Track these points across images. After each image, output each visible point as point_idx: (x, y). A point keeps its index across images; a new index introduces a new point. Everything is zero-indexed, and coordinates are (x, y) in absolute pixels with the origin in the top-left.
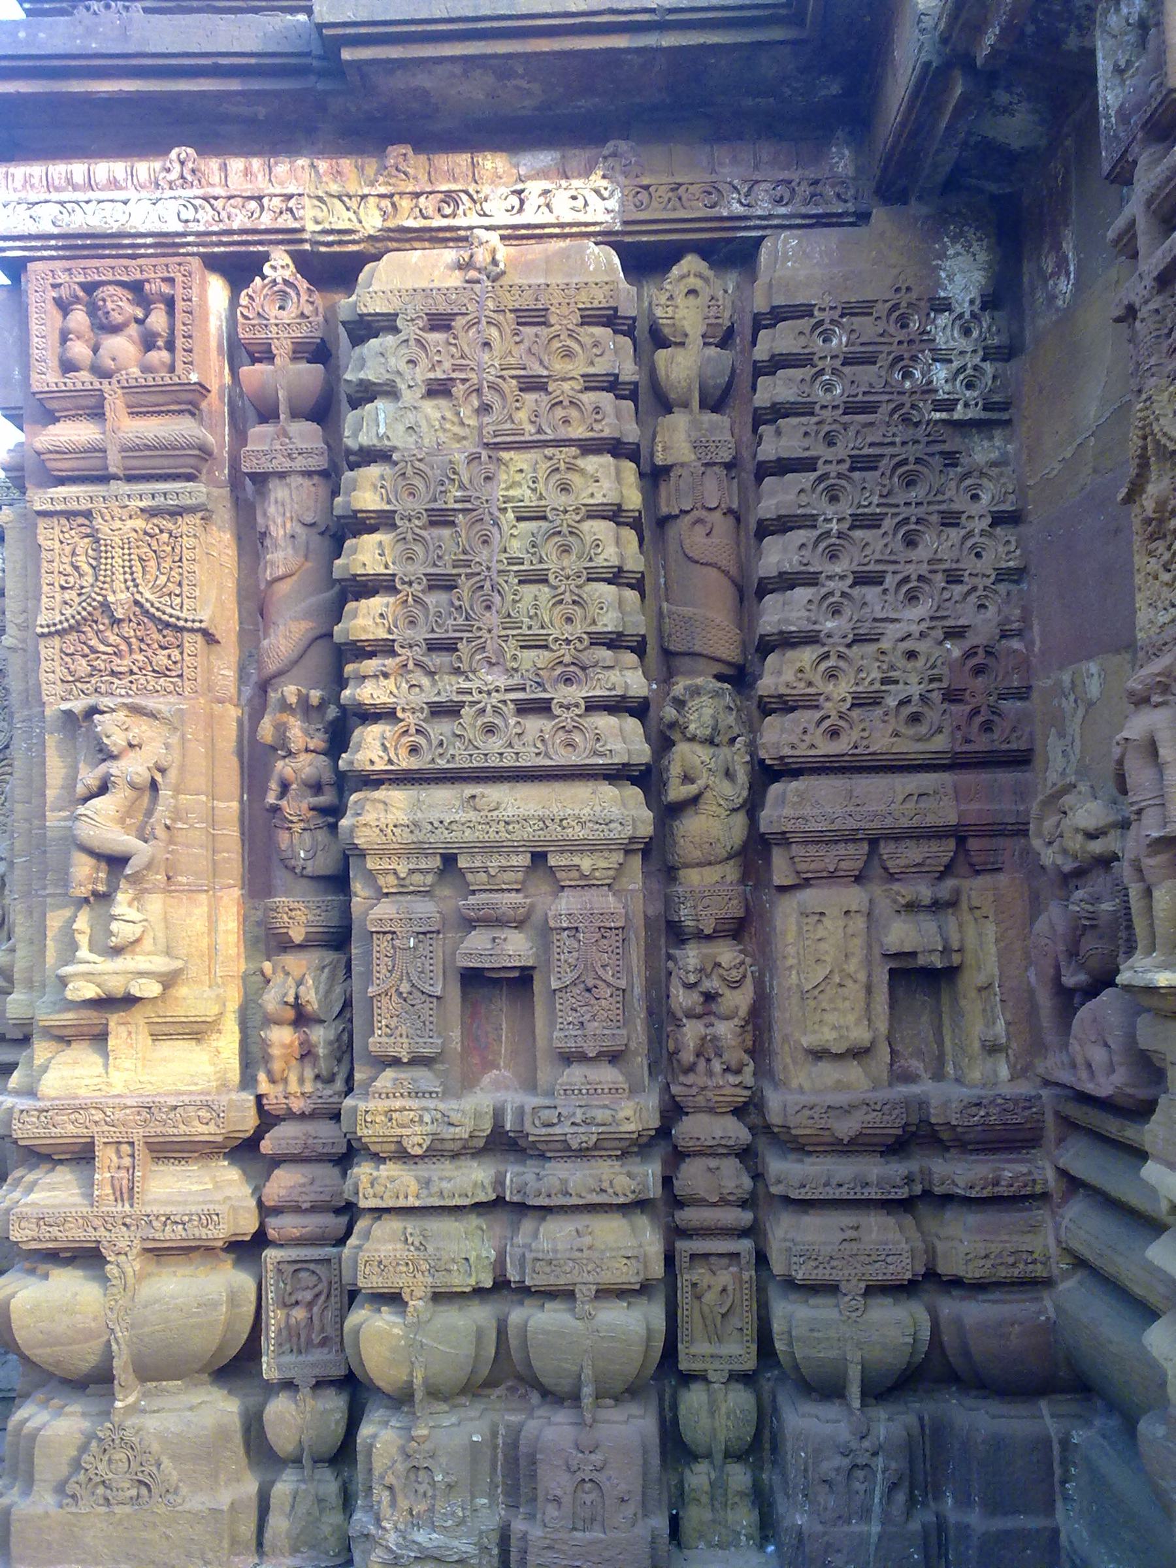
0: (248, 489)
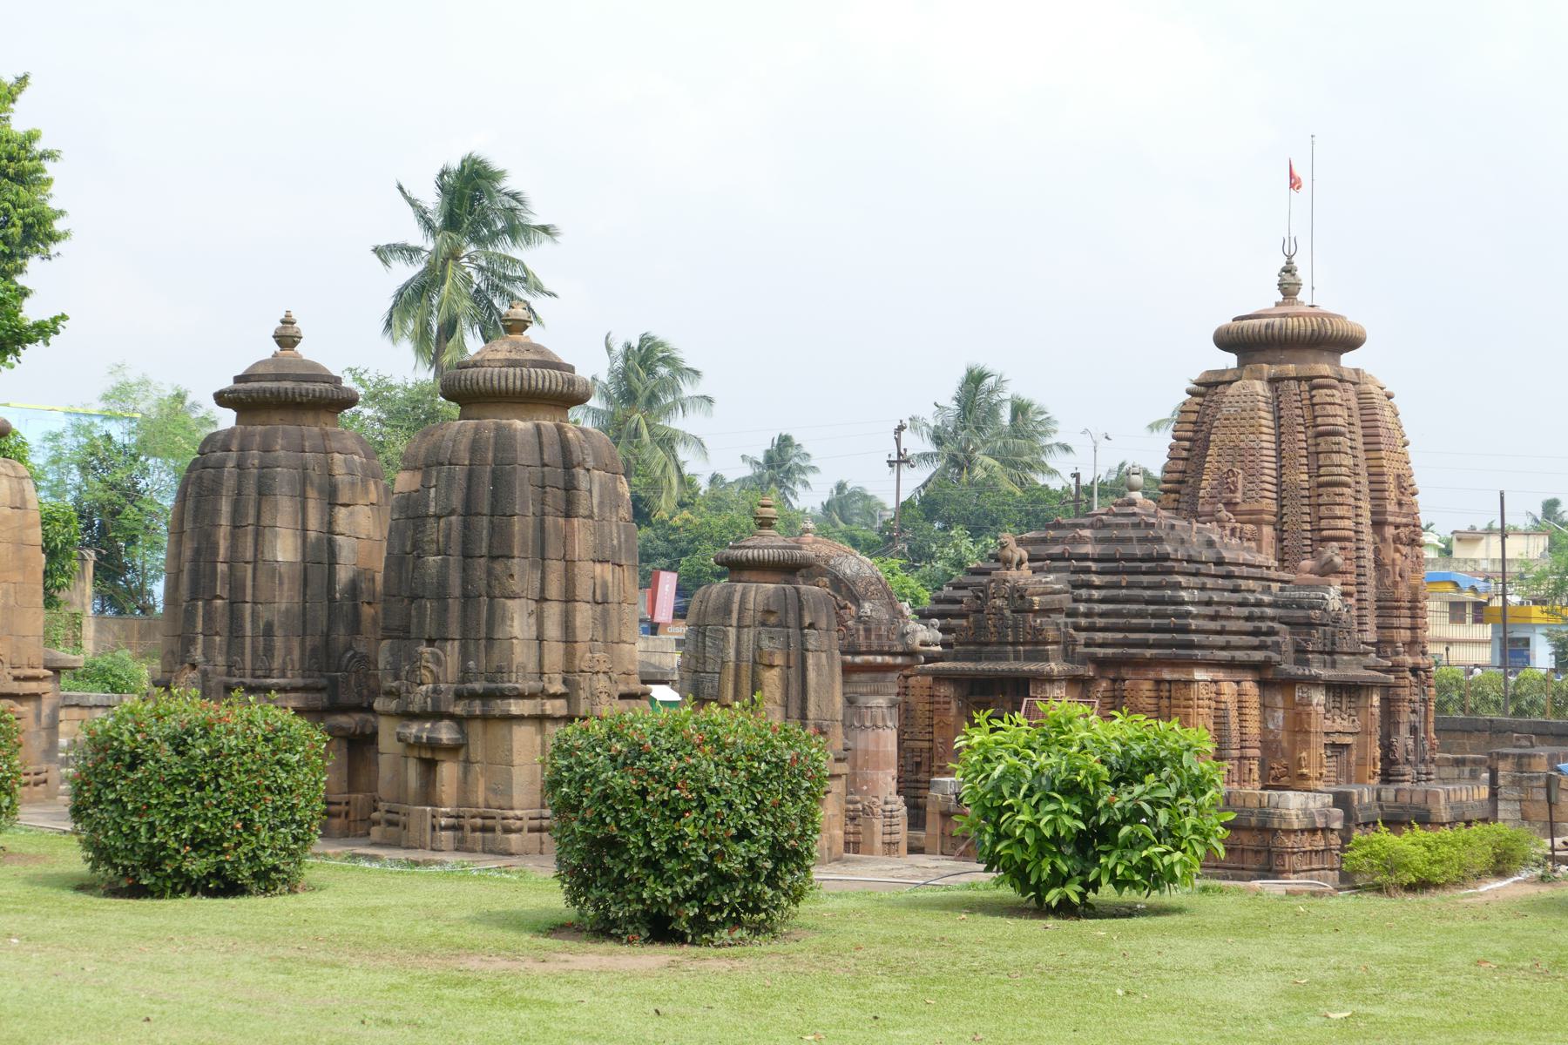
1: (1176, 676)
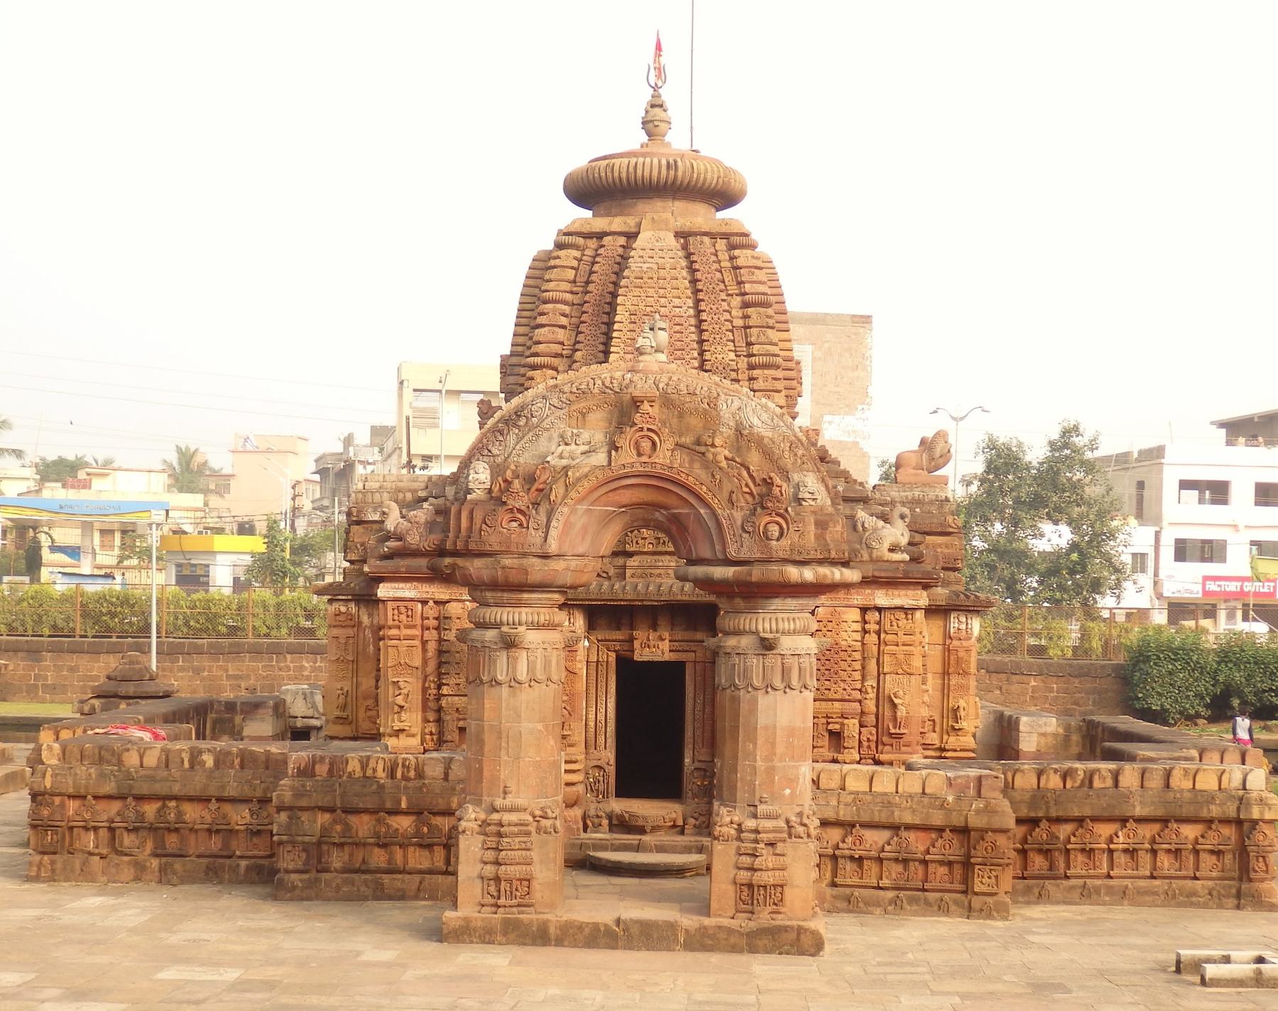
0: (424, 643)
1: (898, 602)
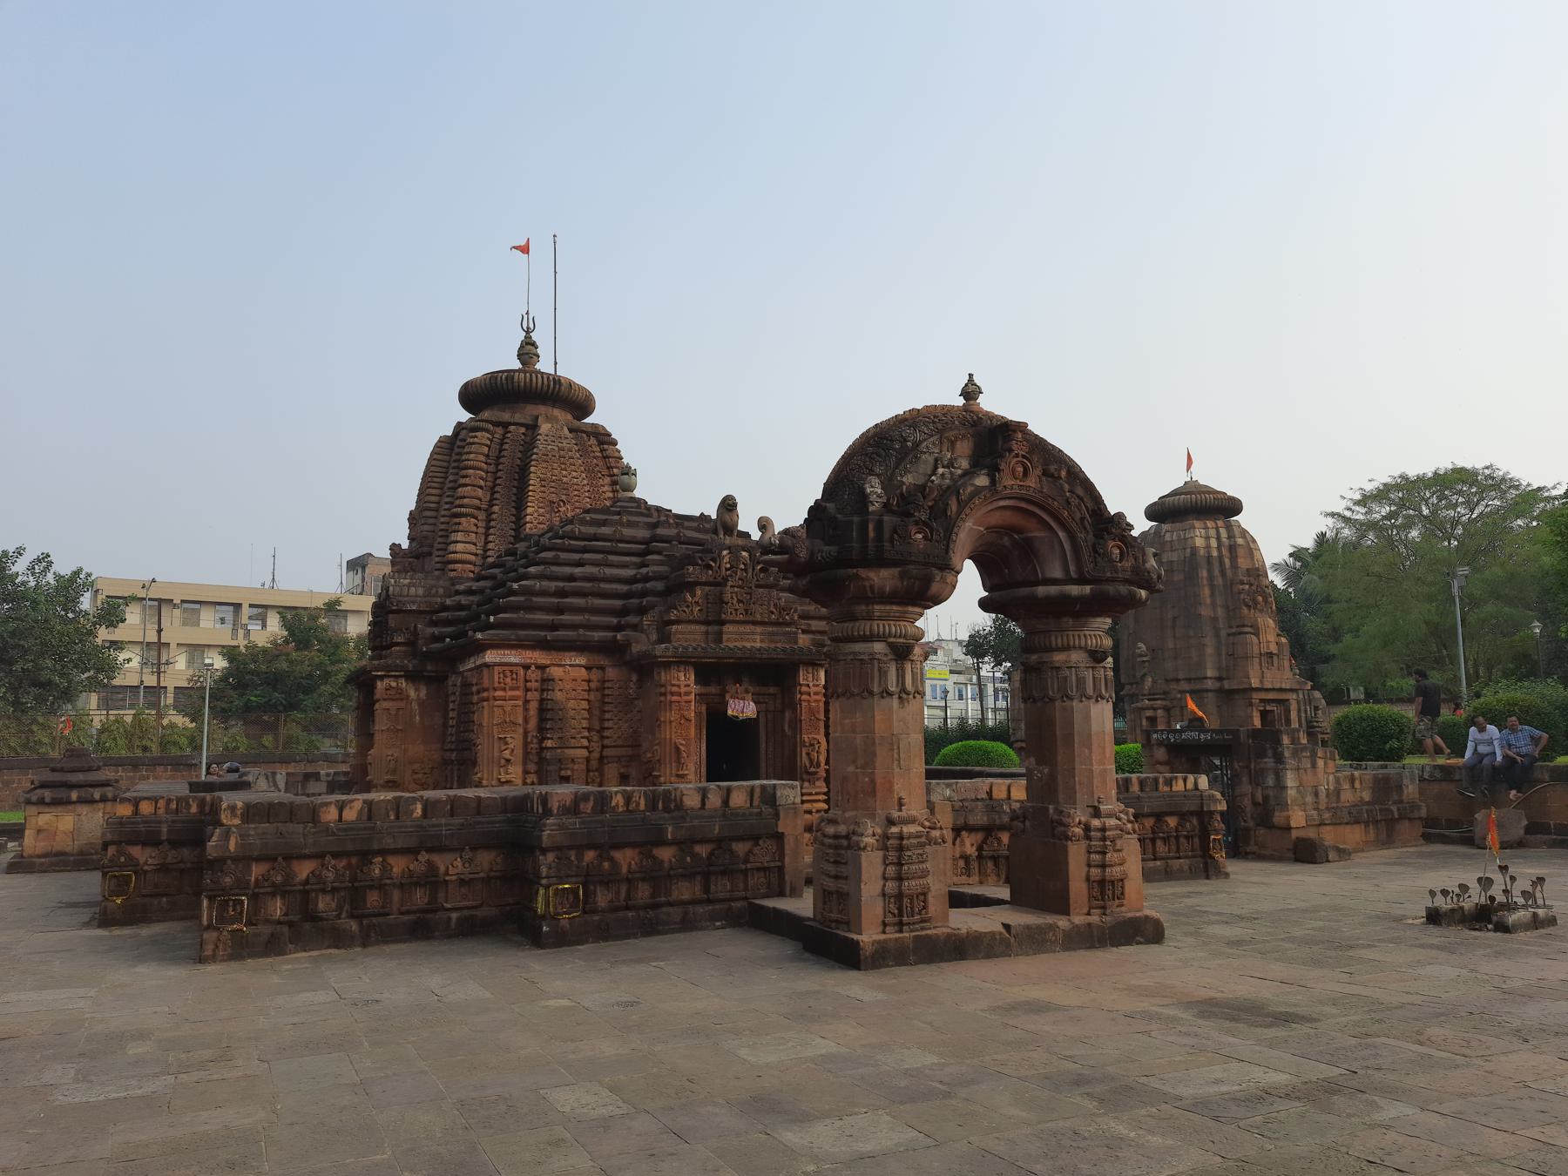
0: (526, 702)
